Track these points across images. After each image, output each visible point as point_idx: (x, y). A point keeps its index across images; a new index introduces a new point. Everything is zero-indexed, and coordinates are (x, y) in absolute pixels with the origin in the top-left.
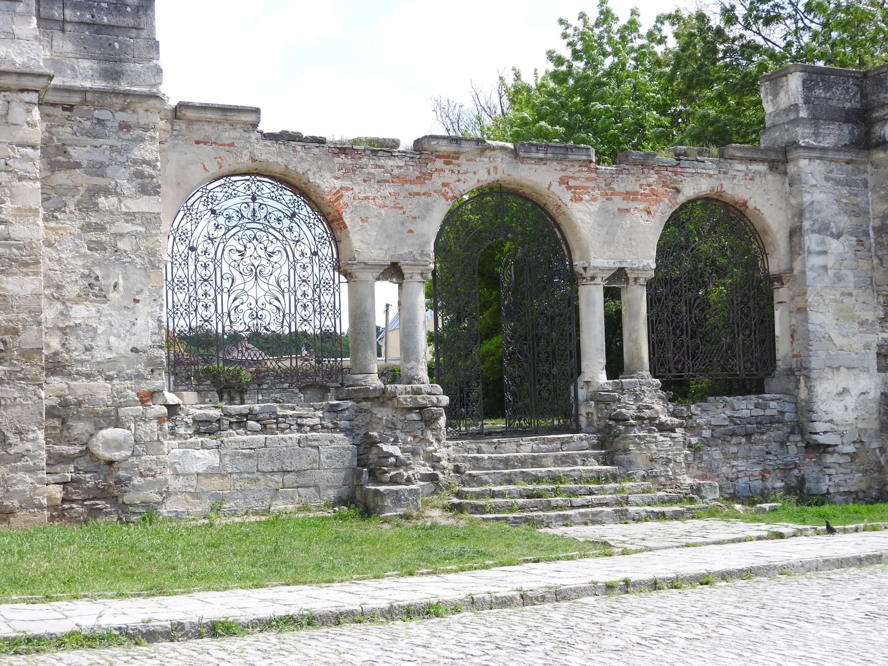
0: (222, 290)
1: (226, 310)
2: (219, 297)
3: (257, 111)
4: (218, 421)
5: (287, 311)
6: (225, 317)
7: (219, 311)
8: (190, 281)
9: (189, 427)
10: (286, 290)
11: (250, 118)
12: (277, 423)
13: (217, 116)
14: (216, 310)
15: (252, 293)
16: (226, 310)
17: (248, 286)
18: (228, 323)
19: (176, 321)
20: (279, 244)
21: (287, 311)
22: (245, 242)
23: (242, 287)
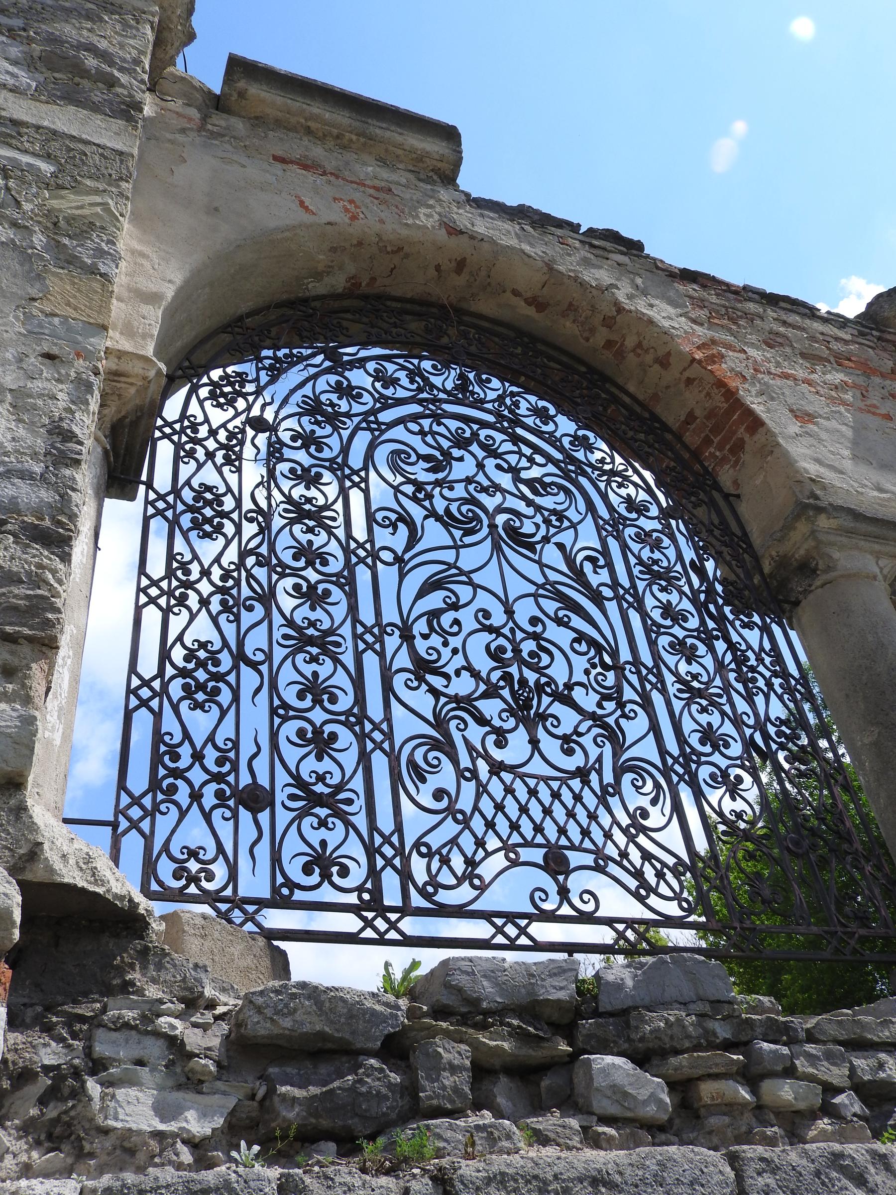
0: (375, 556)
1: (390, 615)
2: (363, 575)
3: (450, 135)
4: (397, 1049)
5: (625, 655)
6: (392, 642)
7: (367, 615)
8: (247, 504)
9: (192, 1083)
10: (607, 592)
11: (434, 147)
12: (752, 1076)
13: (342, 118)
14: (353, 609)
15: (489, 577)
16: (390, 615)
17: (469, 559)
18: (403, 660)
19: (176, 624)
20: (551, 468)
21: (625, 655)
22: (445, 444)
23: (449, 556)
